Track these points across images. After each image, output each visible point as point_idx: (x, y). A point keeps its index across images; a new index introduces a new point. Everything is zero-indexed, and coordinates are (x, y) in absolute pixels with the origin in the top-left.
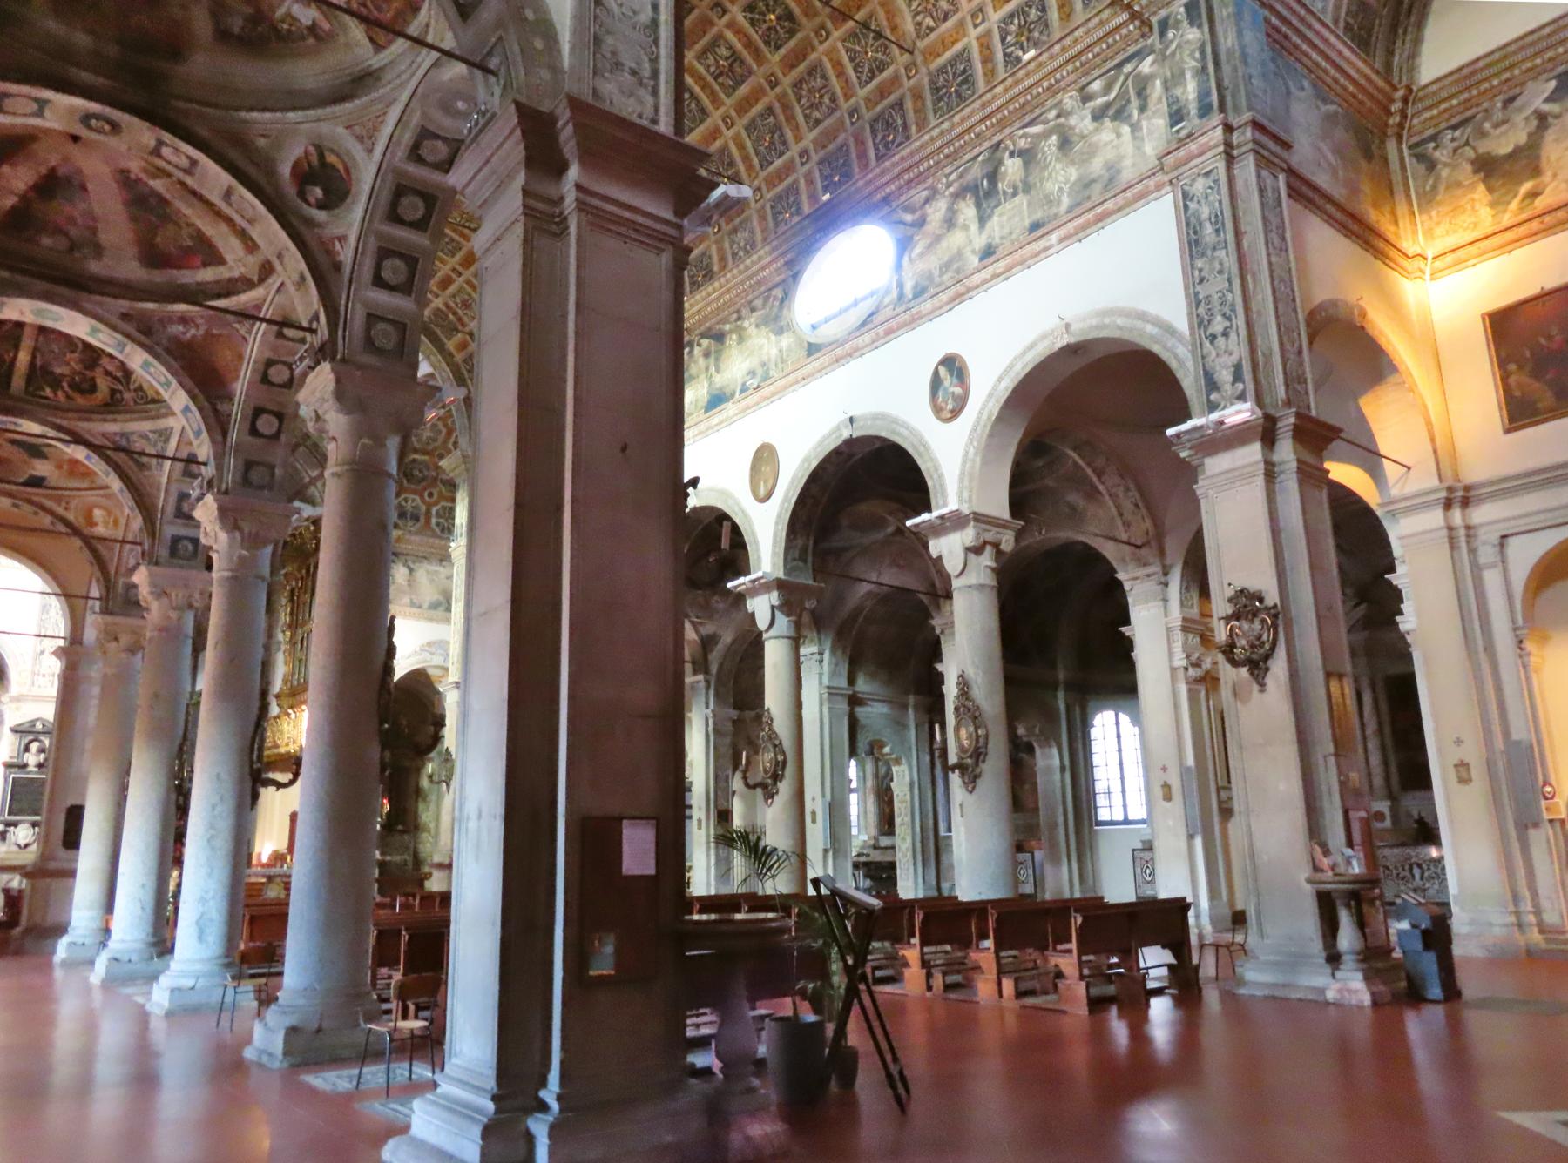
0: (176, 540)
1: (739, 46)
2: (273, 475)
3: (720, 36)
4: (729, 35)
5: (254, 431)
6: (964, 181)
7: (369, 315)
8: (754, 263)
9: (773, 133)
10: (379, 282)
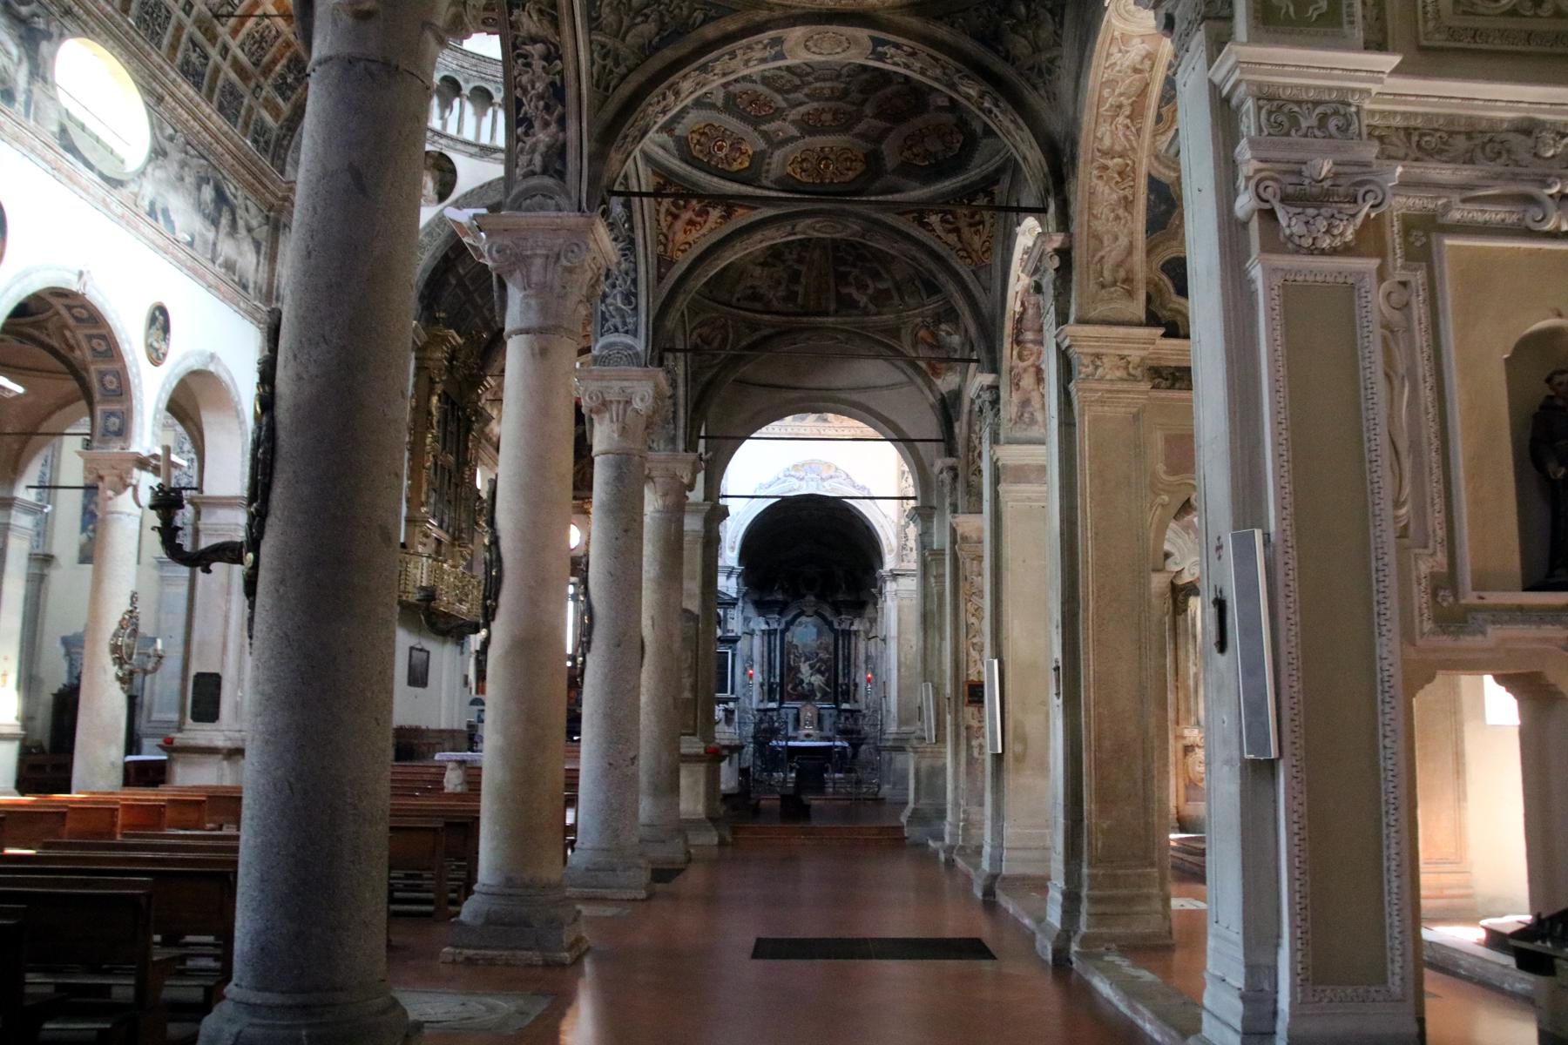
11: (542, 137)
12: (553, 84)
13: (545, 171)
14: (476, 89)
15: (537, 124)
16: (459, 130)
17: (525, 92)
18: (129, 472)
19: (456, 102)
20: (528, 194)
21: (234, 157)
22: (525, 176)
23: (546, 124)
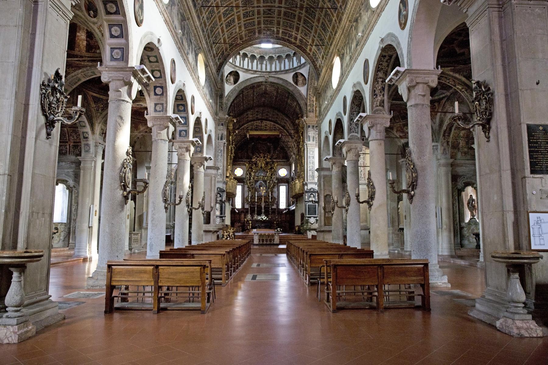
0: (181, 131)
2: (163, 107)
10: (112, 36)
11: (379, 98)
13: (380, 105)
16: (240, 65)
18: (203, 162)
19: (238, 57)
20: (377, 110)
23: (380, 95)
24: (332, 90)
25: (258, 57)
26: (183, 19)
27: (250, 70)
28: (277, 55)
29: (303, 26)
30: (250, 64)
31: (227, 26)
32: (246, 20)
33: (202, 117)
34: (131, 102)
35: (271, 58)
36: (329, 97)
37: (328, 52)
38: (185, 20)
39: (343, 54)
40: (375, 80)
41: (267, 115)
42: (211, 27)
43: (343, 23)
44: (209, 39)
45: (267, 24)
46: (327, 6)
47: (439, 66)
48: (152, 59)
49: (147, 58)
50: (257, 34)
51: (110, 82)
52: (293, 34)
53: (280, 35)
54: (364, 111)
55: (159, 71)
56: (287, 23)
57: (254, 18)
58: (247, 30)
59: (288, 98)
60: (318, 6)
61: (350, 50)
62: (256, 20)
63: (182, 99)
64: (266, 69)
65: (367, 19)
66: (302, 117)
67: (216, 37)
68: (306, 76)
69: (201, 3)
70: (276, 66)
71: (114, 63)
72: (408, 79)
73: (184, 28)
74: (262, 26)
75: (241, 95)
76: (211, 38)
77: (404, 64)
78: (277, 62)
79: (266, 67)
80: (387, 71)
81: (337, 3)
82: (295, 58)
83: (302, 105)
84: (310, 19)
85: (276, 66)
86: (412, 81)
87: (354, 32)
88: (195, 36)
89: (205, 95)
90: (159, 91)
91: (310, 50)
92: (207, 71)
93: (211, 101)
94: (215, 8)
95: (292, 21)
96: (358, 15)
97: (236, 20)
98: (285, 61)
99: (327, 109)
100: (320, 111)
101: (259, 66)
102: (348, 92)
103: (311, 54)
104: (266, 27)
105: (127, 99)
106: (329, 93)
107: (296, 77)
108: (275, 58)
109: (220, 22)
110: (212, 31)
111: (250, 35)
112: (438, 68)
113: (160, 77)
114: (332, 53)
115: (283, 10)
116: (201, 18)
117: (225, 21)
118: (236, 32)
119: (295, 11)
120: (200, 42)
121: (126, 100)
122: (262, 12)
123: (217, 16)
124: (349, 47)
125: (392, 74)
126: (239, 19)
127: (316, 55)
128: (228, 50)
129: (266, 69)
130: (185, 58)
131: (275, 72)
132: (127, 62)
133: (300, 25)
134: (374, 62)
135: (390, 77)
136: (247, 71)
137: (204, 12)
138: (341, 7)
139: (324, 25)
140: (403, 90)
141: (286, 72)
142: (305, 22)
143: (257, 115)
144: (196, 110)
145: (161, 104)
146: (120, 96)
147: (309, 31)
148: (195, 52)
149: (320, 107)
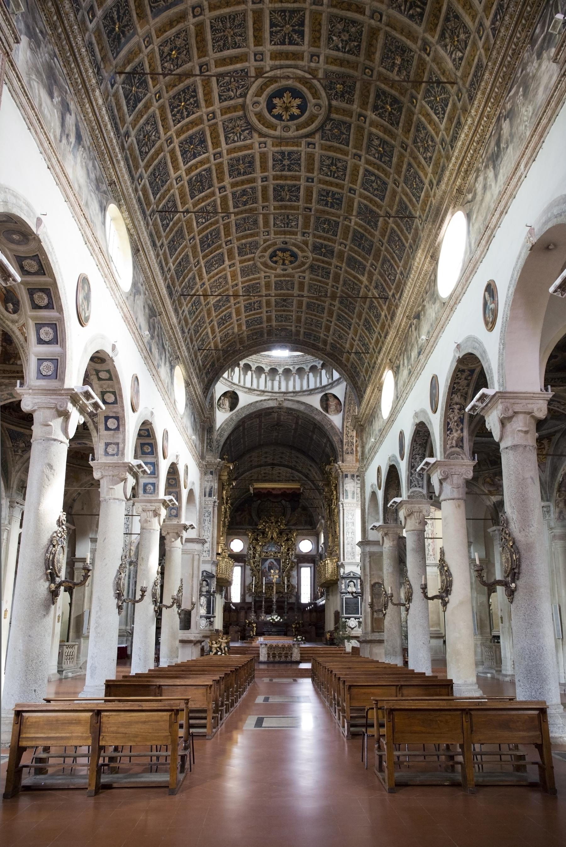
1: (381, 134)
2: (118, 448)
3: (370, 134)
4: (374, 130)
5: (107, 429)
6: (488, 155)
7: (38, 359)
8: (419, 264)
9: (415, 178)
10: (41, 341)
11: (456, 435)
12: (460, 418)
14: (257, 367)
15: (454, 430)
17: (451, 420)
19: (237, 369)
20: (452, 454)
21: (199, 403)
22: (450, 448)
23: (457, 431)
24: (381, 420)
25: (267, 369)
26: (153, 313)
27: (255, 390)
28: (297, 367)
29: (336, 325)
30: (255, 380)
31: (219, 324)
32: (249, 316)
33: (179, 462)
34: (68, 441)
35: (287, 372)
36: (376, 432)
37: (375, 363)
38: (156, 316)
39: (398, 367)
40: (449, 406)
41: (281, 458)
42: (196, 325)
43: (397, 320)
44: (192, 343)
45: (281, 321)
46: (373, 294)
47: (549, 387)
48: (103, 375)
49: (94, 373)
50: (266, 335)
51: (34, 411)
52: (322, 335)
53: (301, 338)
54: (432, 455)
55: (114, 393)
56: (312, 319)
57: (261, 313)
58: (251, 330)
59: (313, 432)
60: (359, 291)
61: (409, 359)
62: (264, 316)
63: (149, 436)
64: (280, 388)
65: (434, 315)
66: (336, 461)
67: (203, 340)
68: (342, 399)
69: (180, 290)
70: (295, 384)
71: (42, 383)
72: (500, 407)
73: (154, 327)
74: (274, 323)
75: (241, 428)
76: (194, 342)
77: (493, 385)
78: (297, 377)
79: (281, 385)
80: (466, 394)
81: (387, 290)
82: (324, 372)
83: (337, 445)
84: (346, 313)
85: (295, 384)
86: (506, 409)
87: (415, 334)
88: (170, 338)
89: (185, 428)
90: (112, 423)
91: (348, 360)
92: (188, 393)
93: (194, 437)
94: (202, 297)
95: (319, 317)
96: (420, 308)
97: (234, 315)
98: (308, 375)
99: (374, 449)
100: (363, 453)
101: (269, 383)
102: (406, 425)
103: (349, 365)
104: (279, 326)
105: (62, 437)
106: (377, 425)
107: (325, 400)
108: (294, 371)
109: (209, 317)
110: (196, 332)
111: (255, 337)
112: (547, 390)
113: (115, 402)
114: (380, 365)
115: (305, 300)
116: (180, 312)
117: (216, 316)
118: (233, 333)
119: (325, 302)
120: (179, 348)
121: (59, 439)
122: (273, 303)
123: (205, 309)
124: (408, 357)
125: (475, 399)
126: (238, 313)
127: (356, 368)
128: (221, 360)
129: (280, 388)
130: (155, 372)
131: (294, 392)
132: (62, 380)
133: (331, 322)
134: (447, 380)
135: (472, 403)
136: (251, 390)
137: (185, 304)
138: (393, 295)
139: (369, 323)
140: (492, 422)
141: (311, 392)
142: (339, 317)
143: (266, 457)
144: (170, 452)
145: (114, 444)
146: (50, 433)
147: (346, 332)
148: (170, 363)
149: (363, 447)
